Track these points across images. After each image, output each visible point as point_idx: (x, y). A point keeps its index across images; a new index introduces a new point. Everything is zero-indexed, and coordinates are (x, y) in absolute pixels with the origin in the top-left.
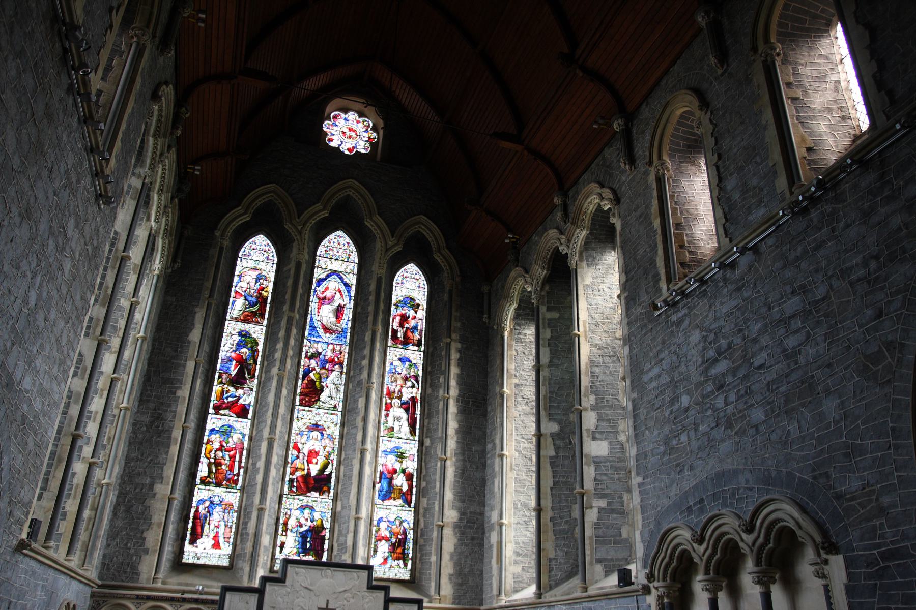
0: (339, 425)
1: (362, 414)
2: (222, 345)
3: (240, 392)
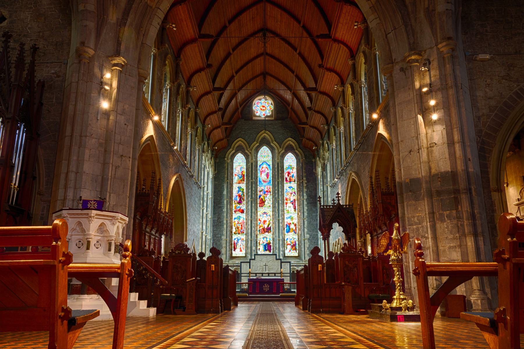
1: (277, 208)
3: (241, 205)
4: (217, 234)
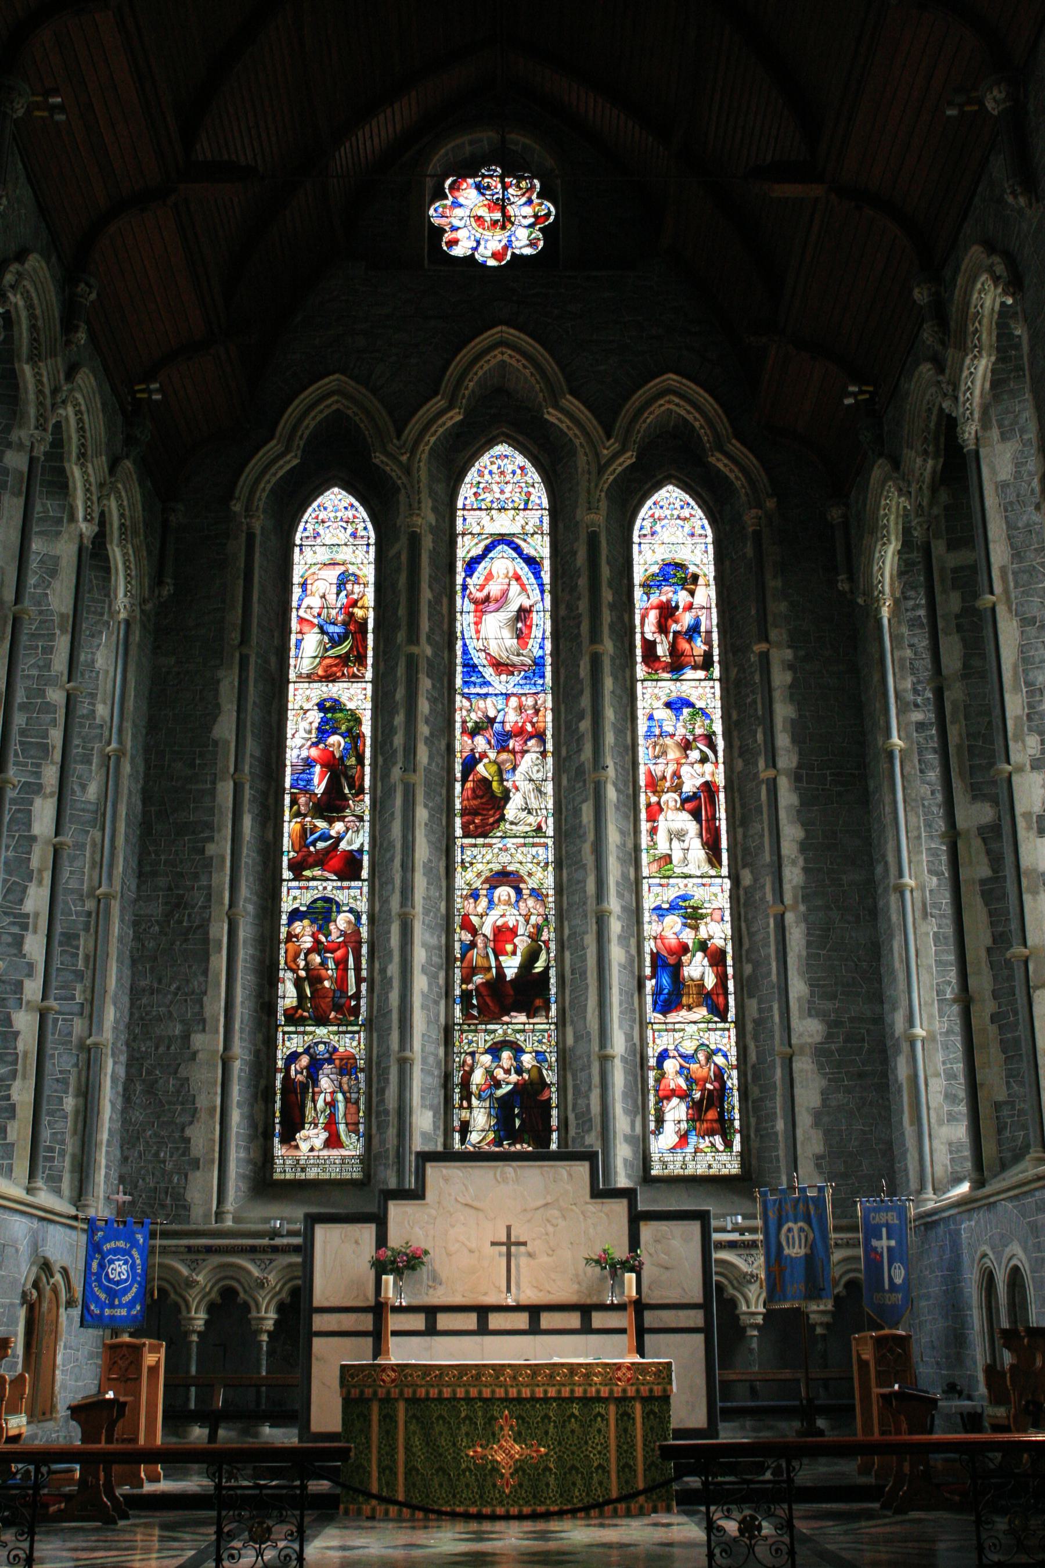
0: (550, 868)
1: (591, 836)
2: (289, 735)
3: (339, 826)
4: (159, 1019)
